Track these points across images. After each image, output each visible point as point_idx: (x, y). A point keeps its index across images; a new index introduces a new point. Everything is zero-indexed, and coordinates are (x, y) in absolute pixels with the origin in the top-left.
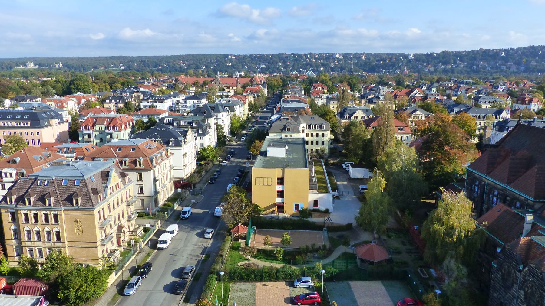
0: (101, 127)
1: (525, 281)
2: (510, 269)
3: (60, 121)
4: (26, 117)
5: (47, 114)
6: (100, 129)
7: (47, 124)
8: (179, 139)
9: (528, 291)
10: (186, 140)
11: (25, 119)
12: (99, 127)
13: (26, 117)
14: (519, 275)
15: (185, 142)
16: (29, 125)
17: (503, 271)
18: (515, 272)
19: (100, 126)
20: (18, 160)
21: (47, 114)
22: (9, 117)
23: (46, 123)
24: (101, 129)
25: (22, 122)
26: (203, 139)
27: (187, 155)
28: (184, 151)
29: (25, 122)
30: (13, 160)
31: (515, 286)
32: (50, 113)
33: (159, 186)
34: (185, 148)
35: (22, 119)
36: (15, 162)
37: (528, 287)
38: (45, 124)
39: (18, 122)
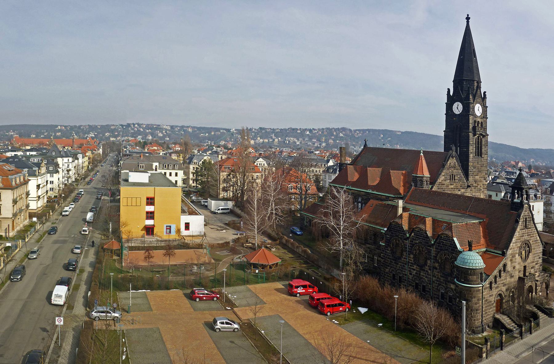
1: (413, 245)
2: (398, 242)
8: (34, 169)
9: (416, 253)
10: (40, 171)
14: (407, 243)
15: (39, 172)
17: (391, 246)
18: (403, 242)
26: (53, 176)
27: (41, 186)
28: (37, 182)
31: (404, 253)
33: (17, 210)
34: (39, 179)
37: (415, 250)
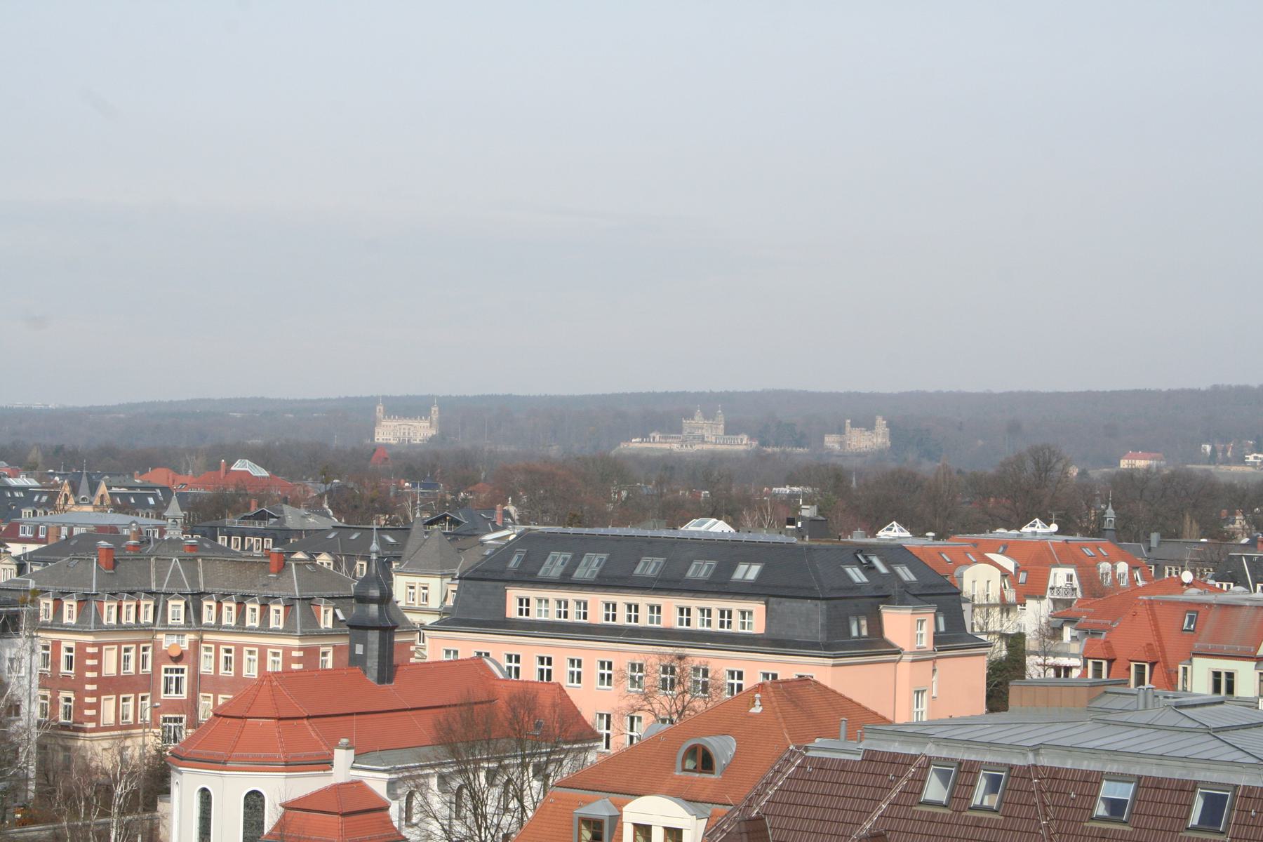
0: (1230, 676)
3: (942, 628)
4: (749, 572)
5: (869, 569)
6: (1217, 689)
7: (864, 632)
11: (738, 583)
12: (1217, 674)
13: (749, 572)
16: (758, 625)
19: (1224, 665)
20: (724, 748)
21: (869, 569)
22: (649, 567)
23: (858, 628)
24: (1230, 689)
25: (716, 605)
29: (735, 606)
30: (692, 752)
32: (886, 563)
35: (721, 586)
36: (706, 762)
38: (855, 633)
39: (694, 604)
